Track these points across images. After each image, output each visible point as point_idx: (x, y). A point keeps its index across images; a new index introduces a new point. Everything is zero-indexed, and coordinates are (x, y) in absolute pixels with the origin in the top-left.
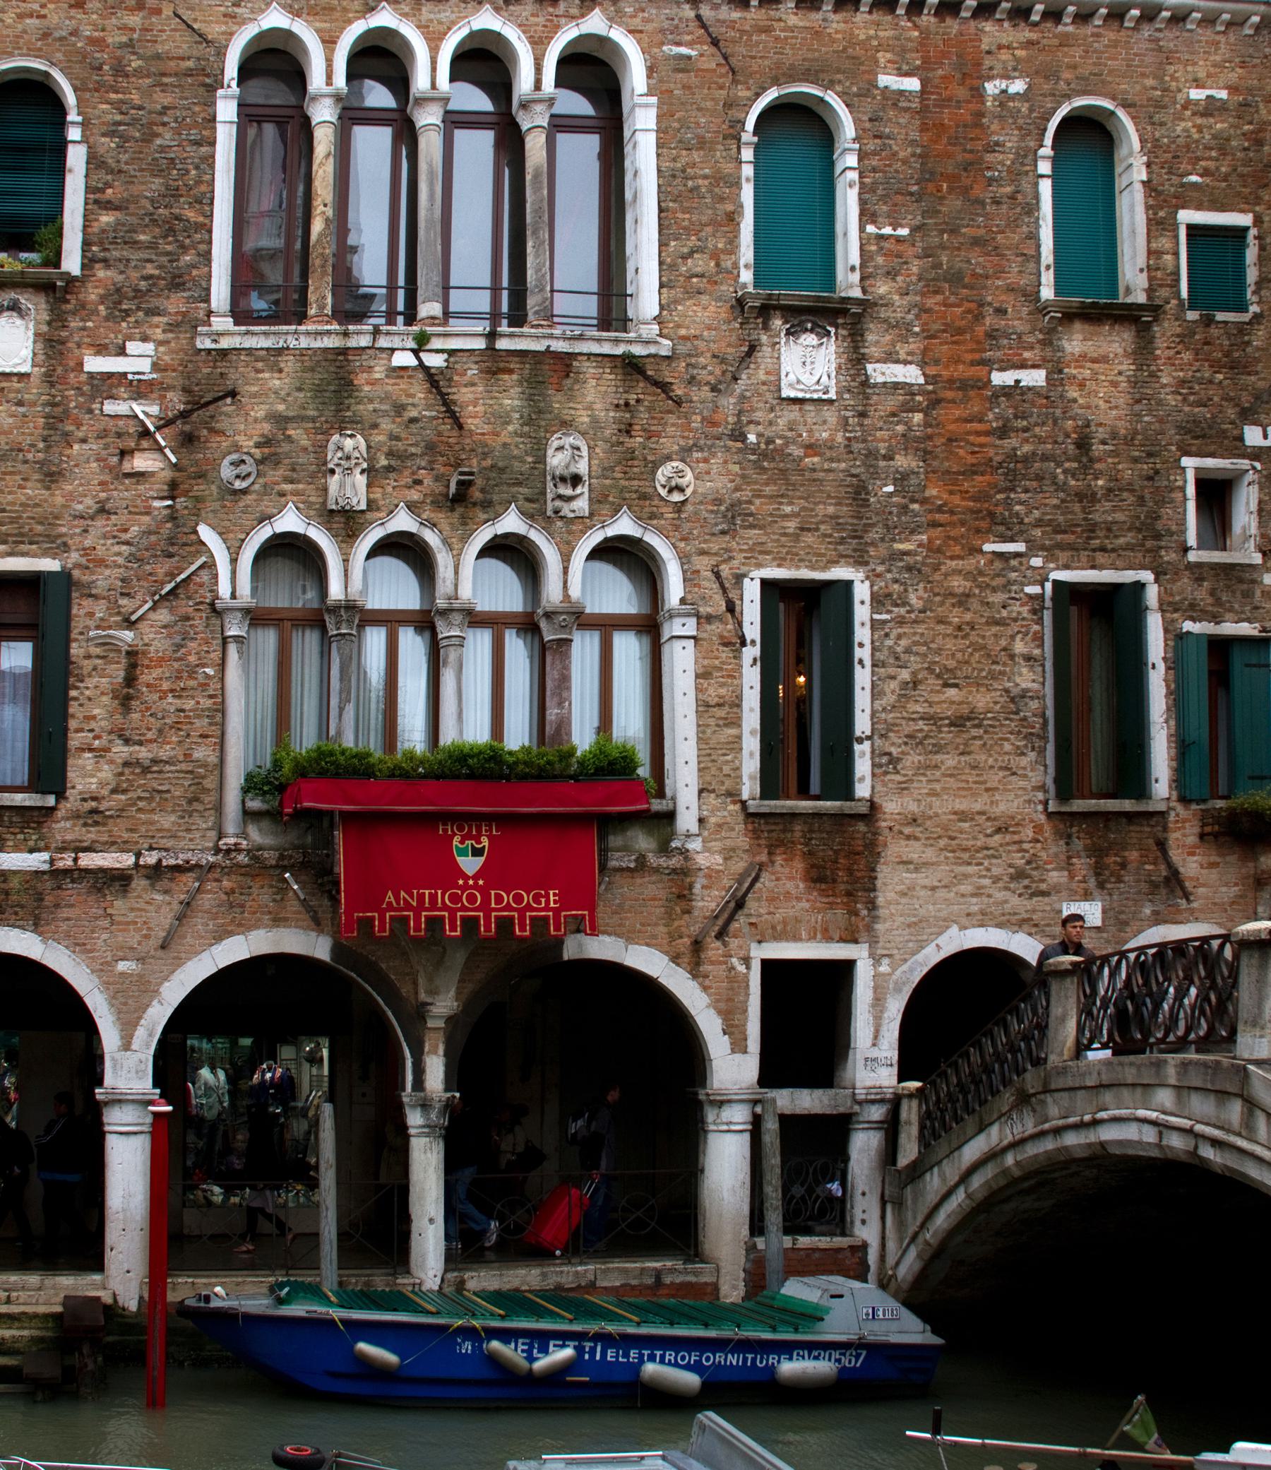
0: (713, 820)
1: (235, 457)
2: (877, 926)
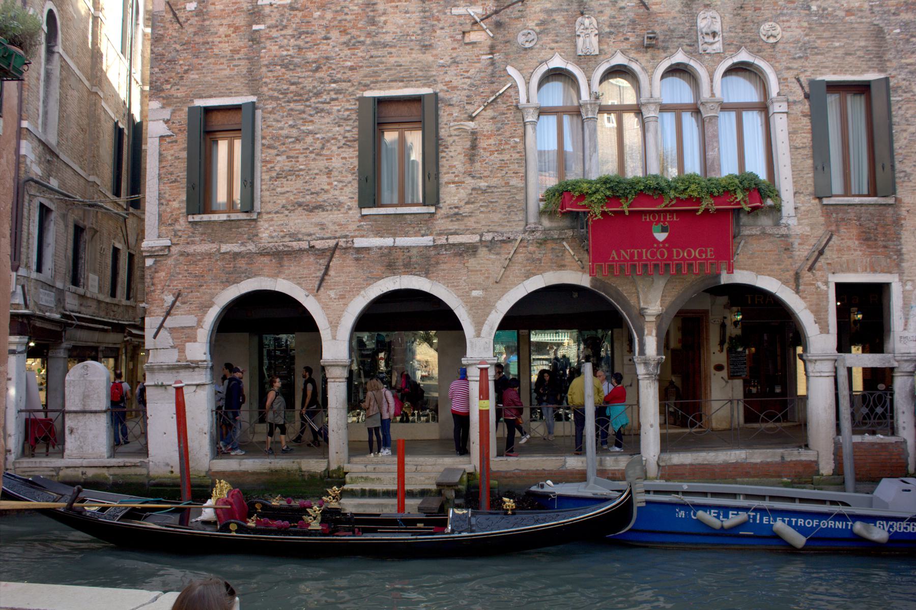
0: (803, 208)
1: (525, 31)
2: (903, 264)
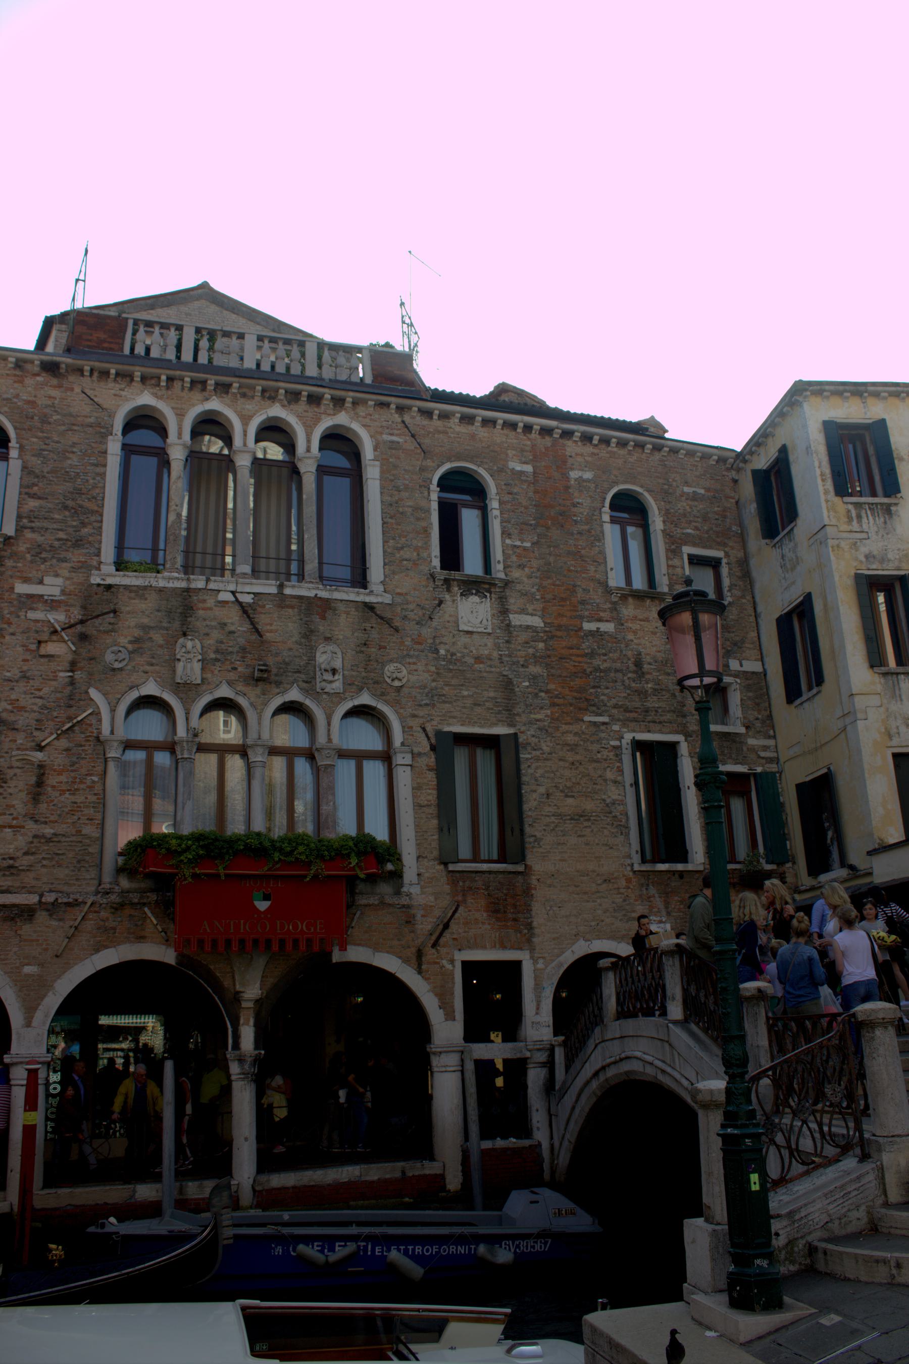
1: (115, 648)
